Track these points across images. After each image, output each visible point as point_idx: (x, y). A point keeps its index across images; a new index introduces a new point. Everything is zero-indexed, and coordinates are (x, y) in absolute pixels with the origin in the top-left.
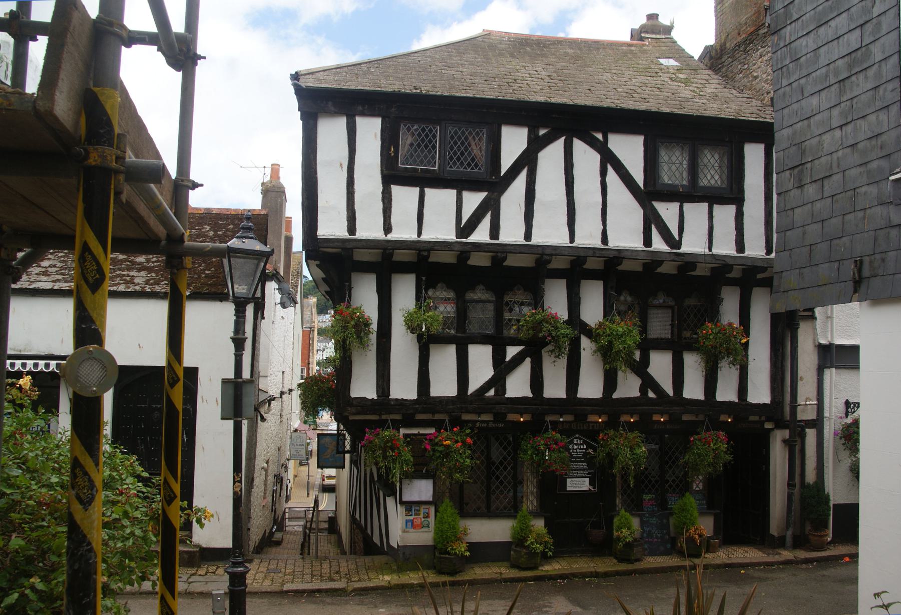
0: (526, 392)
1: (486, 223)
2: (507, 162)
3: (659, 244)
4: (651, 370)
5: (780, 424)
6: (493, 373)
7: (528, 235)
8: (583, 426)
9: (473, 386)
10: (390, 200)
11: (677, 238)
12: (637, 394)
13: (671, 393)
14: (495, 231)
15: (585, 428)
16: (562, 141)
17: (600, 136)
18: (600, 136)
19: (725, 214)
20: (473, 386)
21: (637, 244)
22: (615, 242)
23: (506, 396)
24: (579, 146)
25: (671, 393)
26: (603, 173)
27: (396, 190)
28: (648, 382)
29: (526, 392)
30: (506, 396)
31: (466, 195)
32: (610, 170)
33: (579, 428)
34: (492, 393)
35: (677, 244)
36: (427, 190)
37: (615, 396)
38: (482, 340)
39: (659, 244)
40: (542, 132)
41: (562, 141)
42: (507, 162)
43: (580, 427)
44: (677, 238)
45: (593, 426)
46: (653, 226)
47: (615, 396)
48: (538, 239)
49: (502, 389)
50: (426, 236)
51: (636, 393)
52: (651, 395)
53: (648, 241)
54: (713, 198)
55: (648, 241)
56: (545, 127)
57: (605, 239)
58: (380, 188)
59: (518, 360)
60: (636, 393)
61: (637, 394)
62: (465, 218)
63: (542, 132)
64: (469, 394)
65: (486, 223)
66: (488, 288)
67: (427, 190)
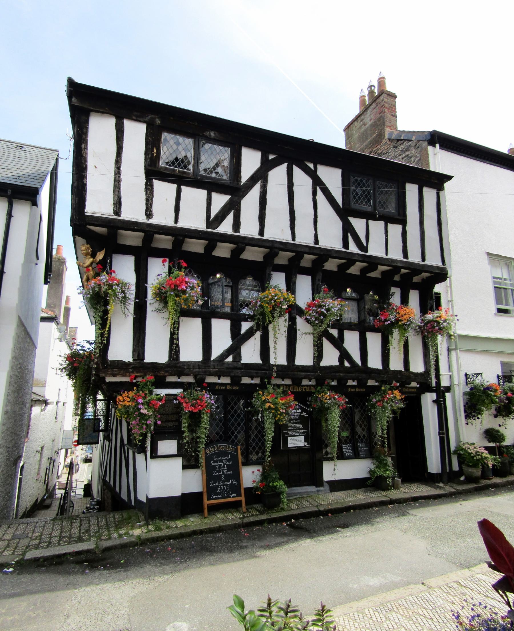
0: (258, 360)
1: (230, 218)
2: (246, 174)
3: (353, 248)
4: (346, 345)
5: (428, 388)
6: (231, 343)
7: (262, 232)
8: (298, 389)
9: (215, 354)
10: (152, 192)
11: (365, 245)
12: (337, 363)
13: (360, 364)
14: (237, 225)
15: (300, 390)
16: (284, 166)
17: (311, 166)
18: (311, 166)
19: (395, 230)
20: (215, 354)
21: (338, 246)
22: (324, 243)
23: (242, 362)
24: (297, 171)
25: (360, 364)
26: (314, 193)
27: (157, 184)
28: (344, 355)
29: (258, 360)
30: (242, 362)
31: (214, 195)
32: (319, 192)
33: (295, 390)
34: (230, 359)
35: (366, 249)
36: (183, 188)
37: (322, 364)
38: (223, 316)
39: (353, 248)
40: (271, 157)
41: (284, 166)
42: (246, 174)
43: (296, 389)
44: (365, 245)
45: (305, 389)
46: (349, 235)
47: (322, 364)
48: (268, 236)
49: (238, 357)
50: (181, 224)
51: (336, 363)
52: (347, 364)
53: (346, 245)
54: (388, 219)
55: (346, 245)
56: (273, 153)
57: (316, 241)
58: (144, 181)
59: (250, 333)
60: (336, 363)
61: (337, 363)
62: (214, 212)
63: (271, 157)
64: (212, 359)
65: (230, 218)
66: (227, 275)
67: (183, 188)
